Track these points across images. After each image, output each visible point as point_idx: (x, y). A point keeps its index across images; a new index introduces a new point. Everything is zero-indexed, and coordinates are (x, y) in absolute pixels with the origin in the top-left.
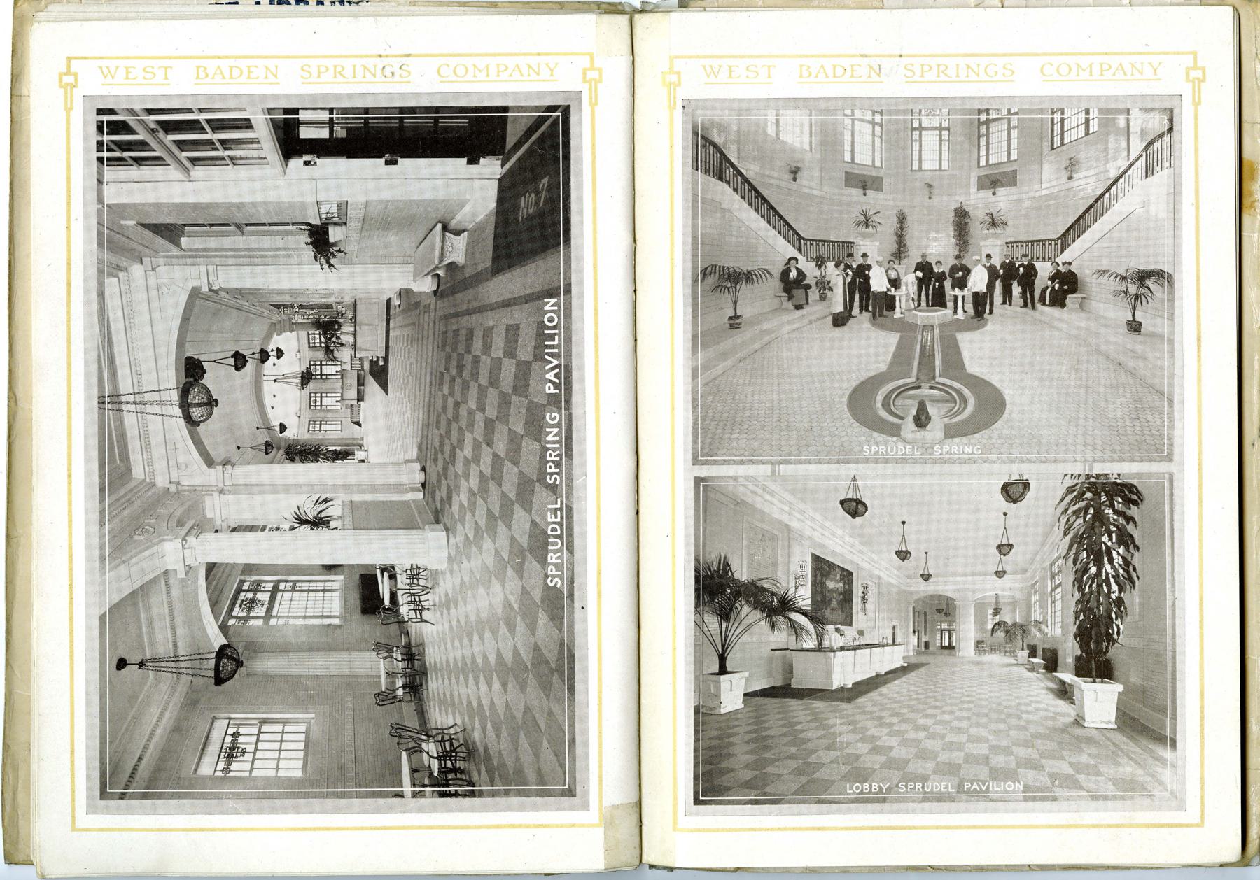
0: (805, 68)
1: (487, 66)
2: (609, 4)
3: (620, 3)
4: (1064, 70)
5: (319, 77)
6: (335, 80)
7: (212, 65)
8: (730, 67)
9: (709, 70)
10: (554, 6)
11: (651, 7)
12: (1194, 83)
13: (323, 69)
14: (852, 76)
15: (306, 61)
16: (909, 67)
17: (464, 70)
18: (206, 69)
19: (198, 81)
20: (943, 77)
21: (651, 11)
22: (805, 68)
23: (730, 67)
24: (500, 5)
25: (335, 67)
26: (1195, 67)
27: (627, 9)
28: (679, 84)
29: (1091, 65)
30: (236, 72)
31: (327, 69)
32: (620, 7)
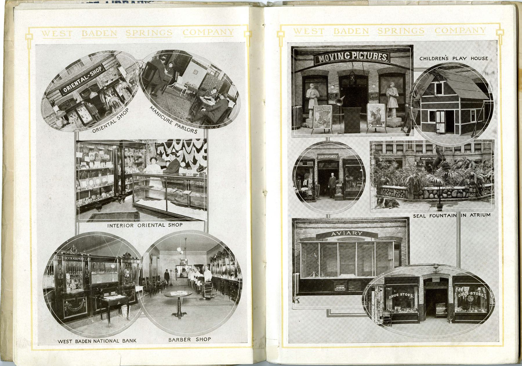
0: (336, 30)
1: (204, 30)
2: (254, 3)
3: (258, 3)
4: (444, 31)
5: (134, 35)
6: (140, 36)
7: (89, 30)
8: (305, 29)
9: (296, 30)
10: (231, 4)
11: (271, 4)
12: (499, 36)
13: (135, 32)
14: (356, 33)
15: (127, 29)
16: (380, 29)
17: (413, 31)
18: (338, 29)
19: (83, 37)
20: (394, 34)
21: (272, 6)
22: (336, 30)
23: (305, 29)
24: (208, 3)
25: (392, 29)
26: (500, 29)
27: (261, 5)
28: (284, 37)
29: (456, 28)
30: (351, 31)
31: (212, 31)
32: (258, 4)
